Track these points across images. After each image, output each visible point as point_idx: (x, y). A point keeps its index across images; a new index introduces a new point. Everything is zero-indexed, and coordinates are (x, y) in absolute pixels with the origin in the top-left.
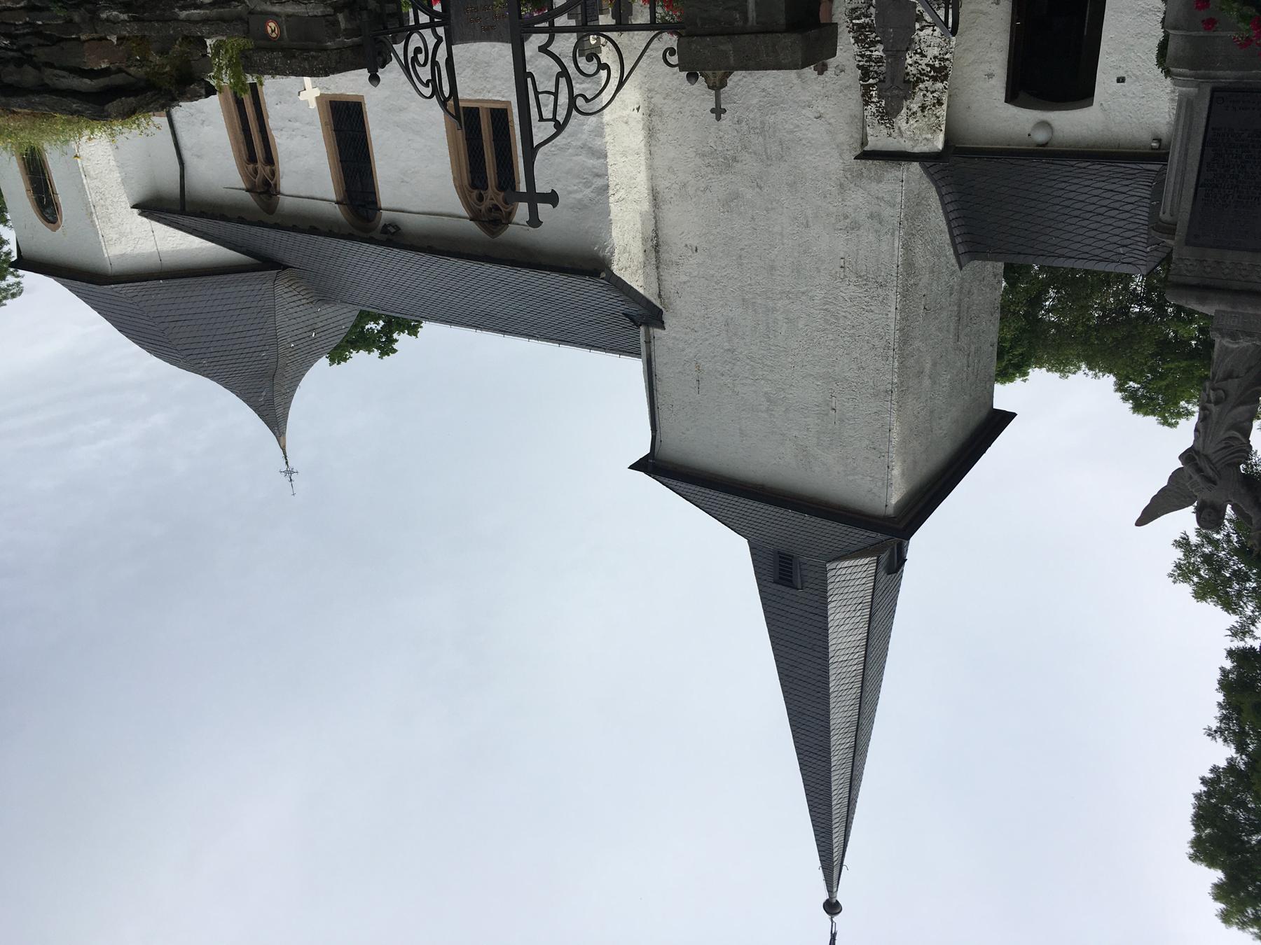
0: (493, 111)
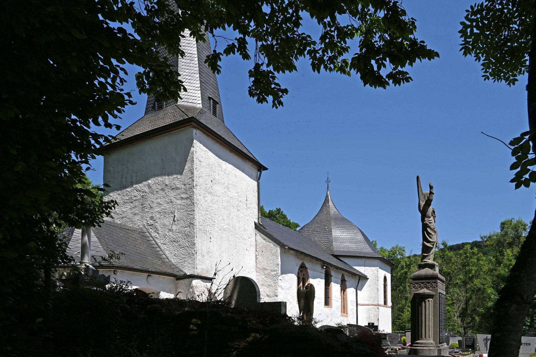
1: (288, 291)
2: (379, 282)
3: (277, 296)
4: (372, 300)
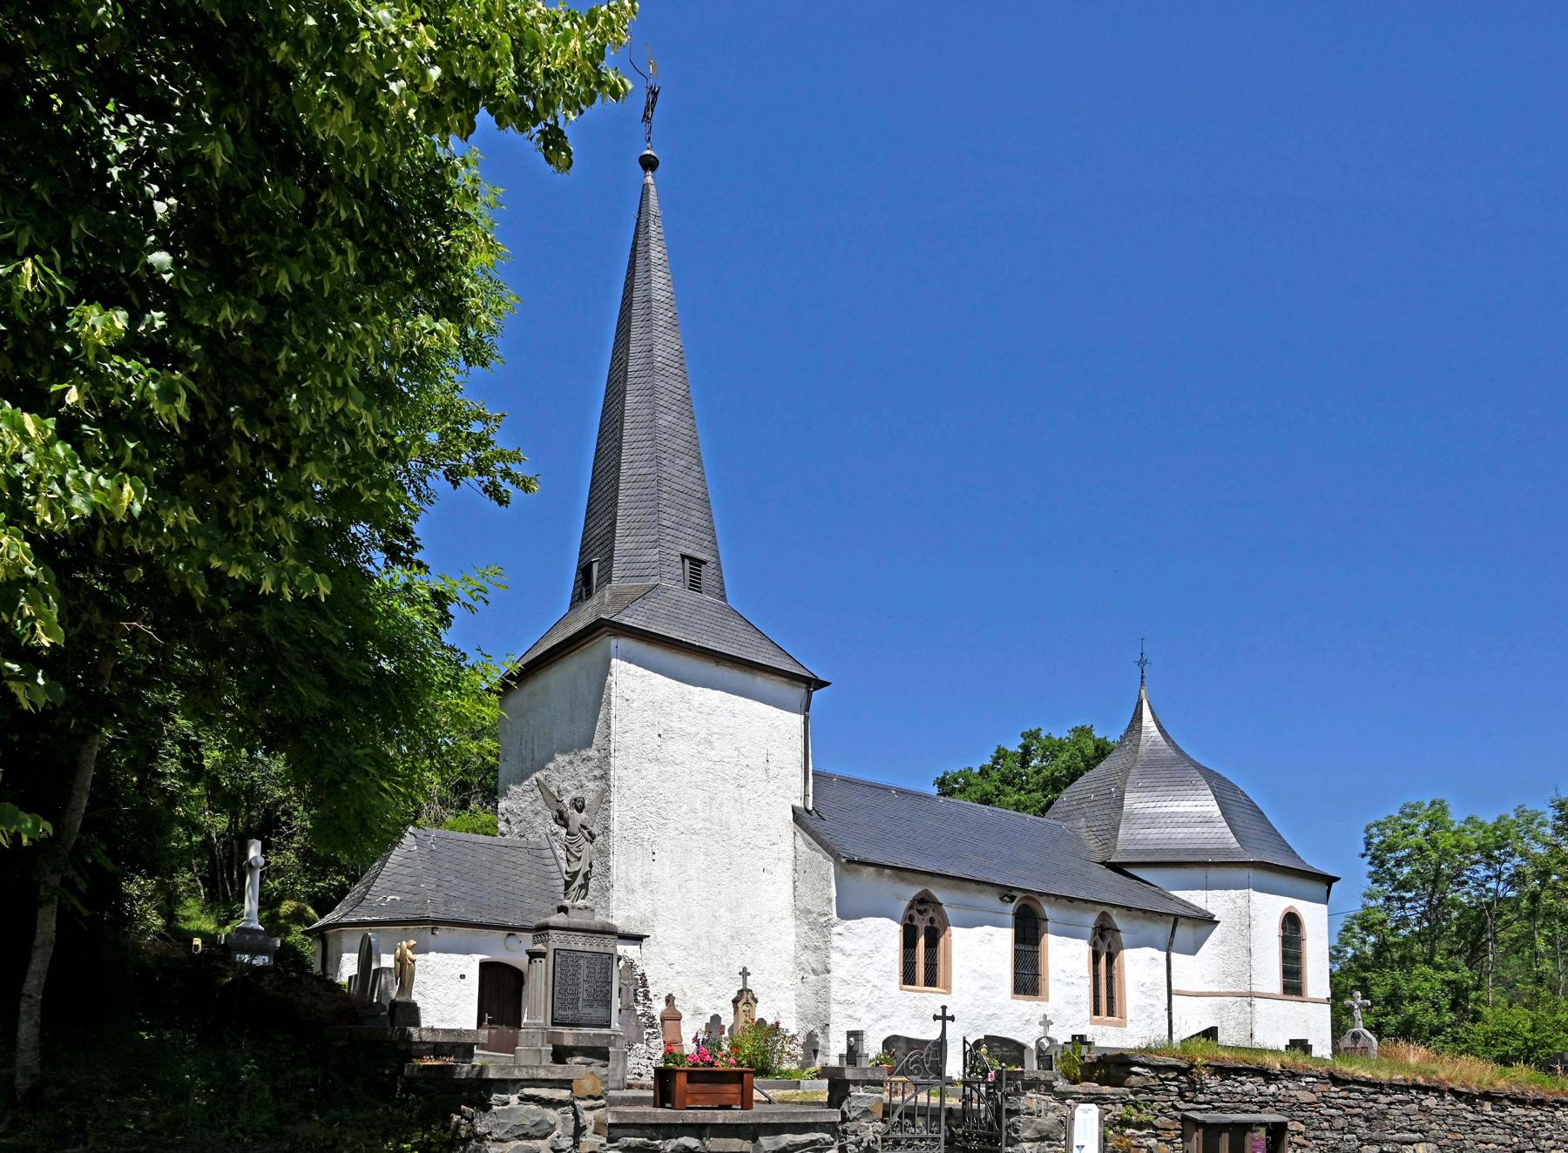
0: (913, 983)
1: (867, 961)
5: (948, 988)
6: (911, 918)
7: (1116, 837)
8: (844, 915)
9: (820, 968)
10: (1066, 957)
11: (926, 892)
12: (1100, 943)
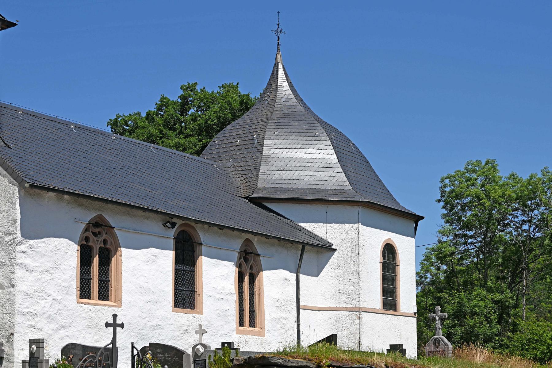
0: (89, 297)
1: (47, 277)
2: (362, 258)
3: (13, 286)
4: (344, 297)
5: (119, 301)
6: (87, 239)
7: (257, 176)
8: (28, 234)
9: (5, 282)
10: (217, 275)
11: (100, 216)
12: (244, 265)
